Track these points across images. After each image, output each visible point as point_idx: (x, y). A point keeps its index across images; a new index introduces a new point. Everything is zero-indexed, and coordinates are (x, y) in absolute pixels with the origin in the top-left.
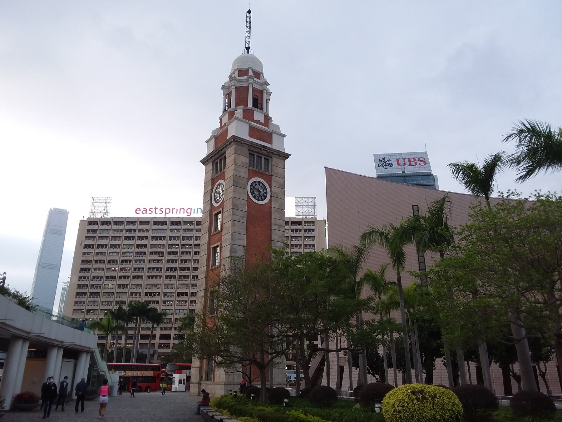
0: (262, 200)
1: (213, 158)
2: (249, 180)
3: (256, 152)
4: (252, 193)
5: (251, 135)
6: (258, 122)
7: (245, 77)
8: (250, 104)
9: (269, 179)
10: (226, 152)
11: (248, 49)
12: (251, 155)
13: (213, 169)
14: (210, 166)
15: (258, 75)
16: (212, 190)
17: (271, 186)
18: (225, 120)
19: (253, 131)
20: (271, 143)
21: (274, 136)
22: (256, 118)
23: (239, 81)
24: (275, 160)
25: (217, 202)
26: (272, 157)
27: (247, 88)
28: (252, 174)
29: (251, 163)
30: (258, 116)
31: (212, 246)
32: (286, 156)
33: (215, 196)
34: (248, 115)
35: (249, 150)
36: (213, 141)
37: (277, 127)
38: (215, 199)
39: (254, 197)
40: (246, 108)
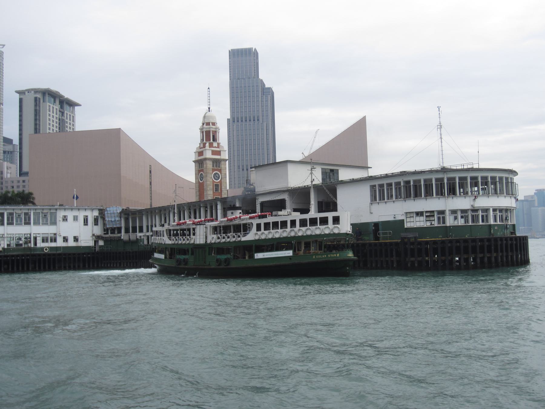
6: (215, 147)
8: (212, 141)
9: (220, 171)
11: (209, 108)
12: (213, 162)
18: (202, 146)
19: (214, 153)
20: (220, 155)
24: (222, 162)
27: (210, 131)
28: (213, 170)
29: (213, 166)
30: (215, 144)
34: (211, 145)
36: (197, 154)
37: (223, 147)
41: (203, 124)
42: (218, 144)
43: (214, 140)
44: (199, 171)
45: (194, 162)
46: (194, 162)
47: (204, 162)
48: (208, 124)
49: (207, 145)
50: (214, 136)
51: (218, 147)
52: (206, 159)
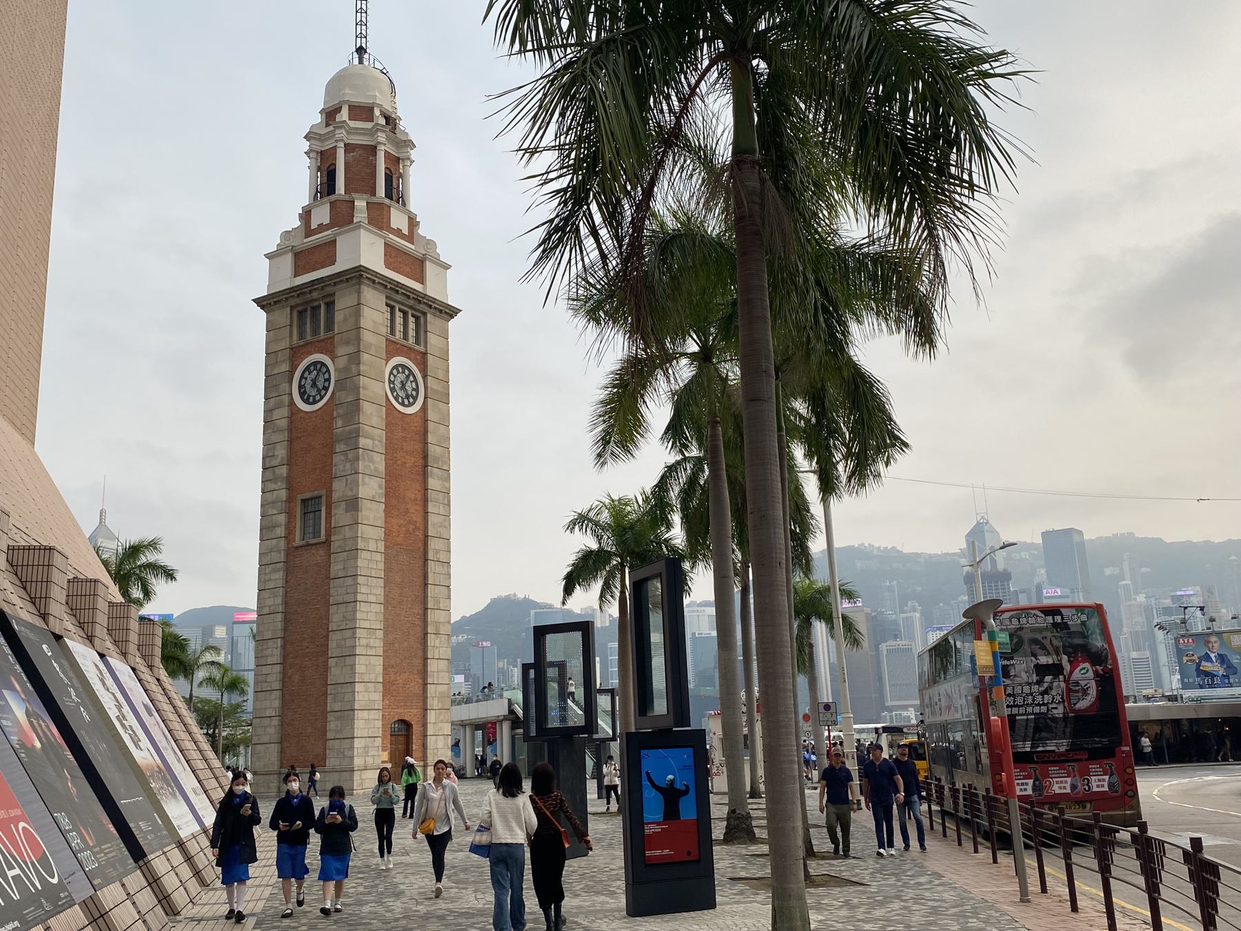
0: (410, 405)
1: (293, 302)
2: (387, 361)
3: (399, 302)
4: (393, 390)
5: (388, 265)
6: (398, 233)
7: (369, 125)
10: (333, 295)
11: (361, 51)
13: (291, 326)
14: (283, 315)
15: (391, 121)
16: (291, 373)
17: (425, 377)
18: (322, 215)
19: (393, 255)
21: (429, 267)
22: (394, 225)
23: (352, 131)
24: (432, 321)
25: (307, 401)
26: (425, 314)
27: (373, 149)
28: (393, 349)
31: (300, 497)
32: (450, 312)
33: (300, 387)
35: (387, 297)
36: (288, 259)
38: (302, 394)
39: (396, 399)
40: (373, 199)
41: (330, 115)
42: (413, 222)
43: (389, 195)
44: (296, 354)
45: (261, 302)
46: (261, 302)
47: (343, 303)
48: (363, 112)
49: (360, 204)
50: (389, 179)
51: (410, 238)
52: (358, 275)
